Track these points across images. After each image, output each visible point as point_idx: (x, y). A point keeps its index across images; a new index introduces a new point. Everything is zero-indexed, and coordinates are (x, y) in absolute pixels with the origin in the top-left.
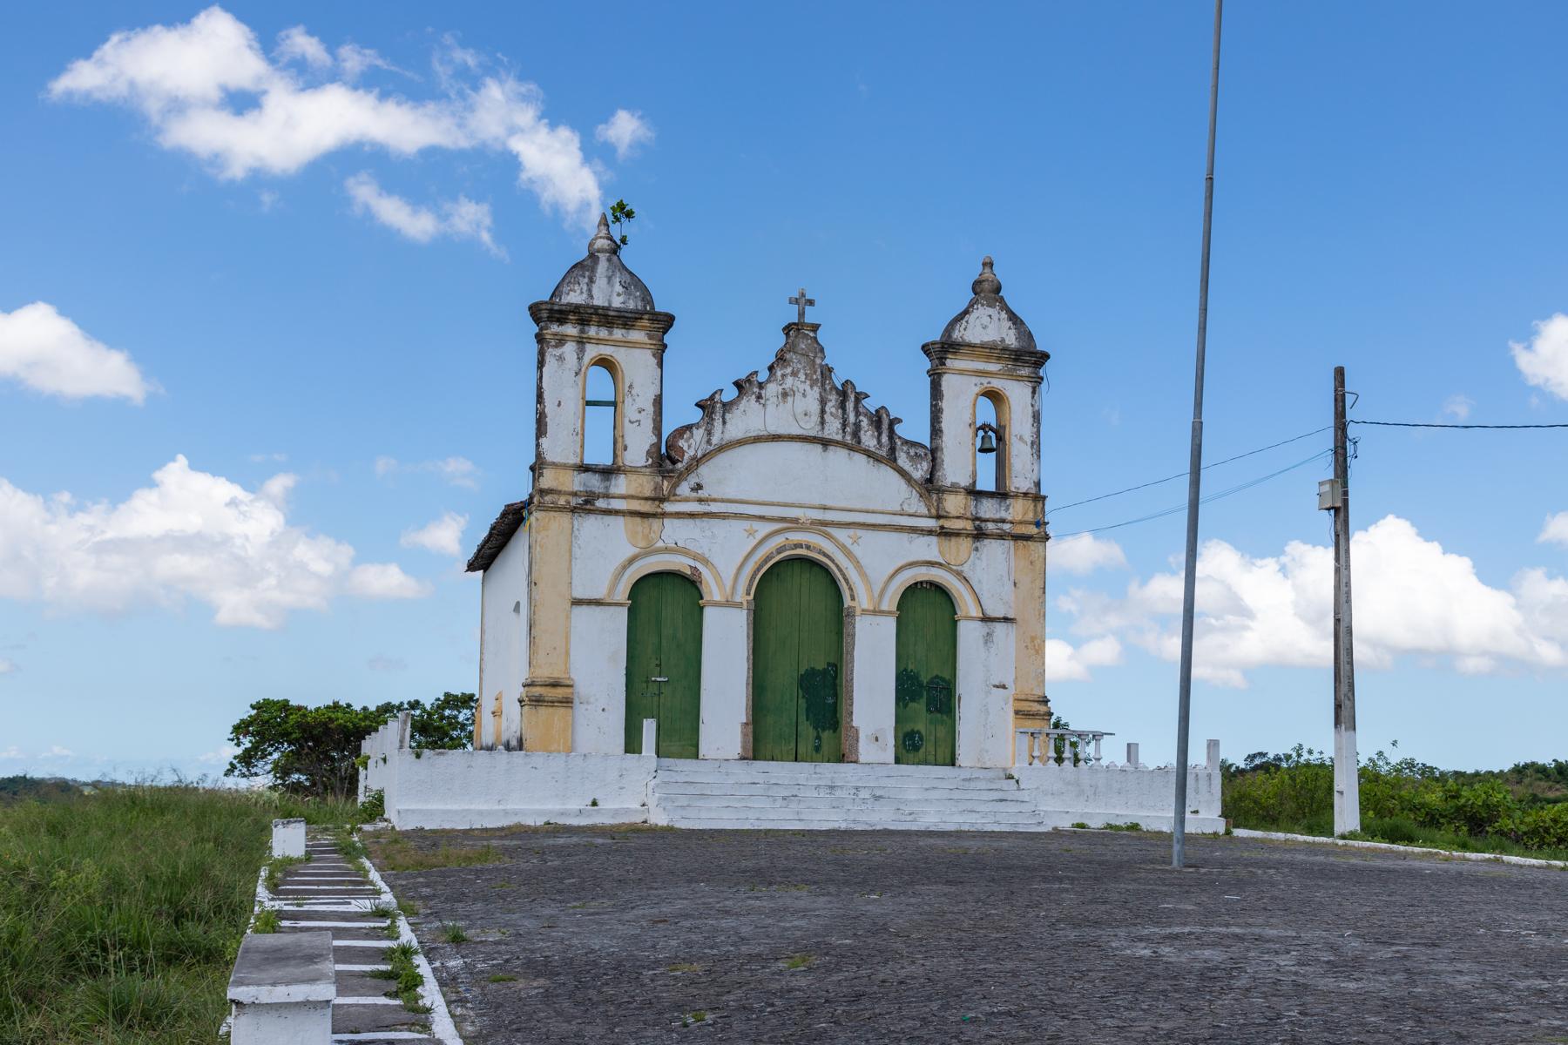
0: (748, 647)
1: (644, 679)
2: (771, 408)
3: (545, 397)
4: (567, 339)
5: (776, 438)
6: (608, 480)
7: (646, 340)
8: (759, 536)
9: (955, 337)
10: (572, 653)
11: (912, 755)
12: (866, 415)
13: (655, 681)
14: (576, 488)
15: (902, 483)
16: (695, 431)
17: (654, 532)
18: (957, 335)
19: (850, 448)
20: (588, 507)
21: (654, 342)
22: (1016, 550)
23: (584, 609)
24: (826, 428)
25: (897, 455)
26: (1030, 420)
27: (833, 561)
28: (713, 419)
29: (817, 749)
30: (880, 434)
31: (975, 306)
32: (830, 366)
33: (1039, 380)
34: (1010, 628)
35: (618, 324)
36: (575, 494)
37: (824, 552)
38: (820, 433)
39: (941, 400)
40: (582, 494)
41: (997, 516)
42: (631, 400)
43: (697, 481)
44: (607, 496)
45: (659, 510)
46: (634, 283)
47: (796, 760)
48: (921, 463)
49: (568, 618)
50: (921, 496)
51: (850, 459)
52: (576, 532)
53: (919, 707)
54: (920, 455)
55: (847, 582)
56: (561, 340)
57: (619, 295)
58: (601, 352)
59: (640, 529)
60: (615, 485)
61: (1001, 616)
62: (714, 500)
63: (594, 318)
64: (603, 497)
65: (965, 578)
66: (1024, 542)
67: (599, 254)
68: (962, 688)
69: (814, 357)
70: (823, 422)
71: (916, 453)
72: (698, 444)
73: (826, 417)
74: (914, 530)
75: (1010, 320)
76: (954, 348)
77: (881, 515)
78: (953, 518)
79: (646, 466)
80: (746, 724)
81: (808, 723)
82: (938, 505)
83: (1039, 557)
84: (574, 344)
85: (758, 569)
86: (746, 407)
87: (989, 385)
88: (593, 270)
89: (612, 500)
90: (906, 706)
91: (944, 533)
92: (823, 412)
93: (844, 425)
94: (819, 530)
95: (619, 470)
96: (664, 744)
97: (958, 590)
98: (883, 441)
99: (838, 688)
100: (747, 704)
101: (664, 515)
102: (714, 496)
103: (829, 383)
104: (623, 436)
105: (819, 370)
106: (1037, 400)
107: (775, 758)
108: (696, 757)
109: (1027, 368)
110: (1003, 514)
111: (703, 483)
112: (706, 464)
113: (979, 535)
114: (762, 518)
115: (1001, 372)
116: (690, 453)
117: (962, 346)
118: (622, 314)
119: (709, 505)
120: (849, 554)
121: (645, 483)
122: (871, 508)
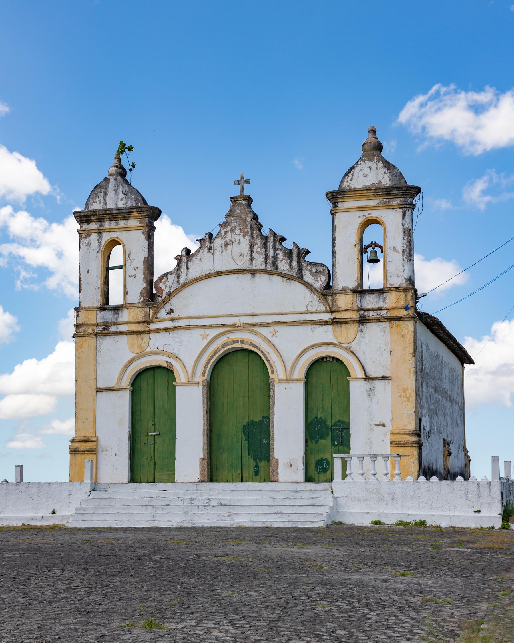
0: (204, 409)
1: (145, 434)
2: (217, 254)
5: (219, 274)
6: (117, 314)
7: (138, 224)
8: (210, 338)
9: (344, 186)
10: (98, 420)
13: (152, 435)
14: (99, 321)
17: (144, 342)
18: (345, 185)
19: (270, 273)
20: (106, 332)
21: (142, 225)
22: (391, 328)
23: (104, 394)
24: (254, 261)
25: (303, 273)
26: (402, 235)
27: (259, 349)
28: (180, 267)
29: (256, 473)
30: (291, 261)
31: (359, 163)
34: (387, 383)
35: (120, 218)
36: (97, 325)
37: (253, 344)
38: (250, 266)
41: (377, 306)
42: (129, 263)
43: (171, 308)
44: (116, 324)
47: (242, 482)
48: (321, 277)
49: (95, 400)
50: (320, 299)
51: (270, 280)
52: (99, 348)
53: (327, 442)
54: (320, 271)
55: (269, 362)
57: (122, 200)
59: (136, 341)
60: (121, 316)
61: (381, 376)
62: (181, 318)
63: (106, 217)
64: (114, 325)
65: (352, 352)
66: (397, 322)
70: (252, 259)
71: (317, 270)
72: (171, 285)
73: (255, 255)
74: (314, 323)
75: (385, 167)
76: (341, 195)
78: (342, 311)
79: (140, 303)
80: (203, 459)
81: (250, 456)
82: (333, 303)
83: (408, 331)
85: (210, 360)
86: (201, 256)
87: (369, 216)
88: (106, 187)
89: (119, 326)
91: (335, 322)
92: (252, 252)
93: (266, 259)
94: (249, 330)
95: (122, 307)
96: (158, 474)
97: (348, 360)
98: (293, 265)
100: (204, 447)
101: (149, 331)
102: (182, 316)
103: (256, 232)
105: (249, 225)
107: (228, 481)
108: (173, 481)
110: (381, 304)
112: (176, 296)
113: (362, 321)
114: (210, 326)
115: (377, 205)
116: (166, 291)
117: (345, 192)
118: (121, 211)
121: (139, 313)
122: (285, 311)
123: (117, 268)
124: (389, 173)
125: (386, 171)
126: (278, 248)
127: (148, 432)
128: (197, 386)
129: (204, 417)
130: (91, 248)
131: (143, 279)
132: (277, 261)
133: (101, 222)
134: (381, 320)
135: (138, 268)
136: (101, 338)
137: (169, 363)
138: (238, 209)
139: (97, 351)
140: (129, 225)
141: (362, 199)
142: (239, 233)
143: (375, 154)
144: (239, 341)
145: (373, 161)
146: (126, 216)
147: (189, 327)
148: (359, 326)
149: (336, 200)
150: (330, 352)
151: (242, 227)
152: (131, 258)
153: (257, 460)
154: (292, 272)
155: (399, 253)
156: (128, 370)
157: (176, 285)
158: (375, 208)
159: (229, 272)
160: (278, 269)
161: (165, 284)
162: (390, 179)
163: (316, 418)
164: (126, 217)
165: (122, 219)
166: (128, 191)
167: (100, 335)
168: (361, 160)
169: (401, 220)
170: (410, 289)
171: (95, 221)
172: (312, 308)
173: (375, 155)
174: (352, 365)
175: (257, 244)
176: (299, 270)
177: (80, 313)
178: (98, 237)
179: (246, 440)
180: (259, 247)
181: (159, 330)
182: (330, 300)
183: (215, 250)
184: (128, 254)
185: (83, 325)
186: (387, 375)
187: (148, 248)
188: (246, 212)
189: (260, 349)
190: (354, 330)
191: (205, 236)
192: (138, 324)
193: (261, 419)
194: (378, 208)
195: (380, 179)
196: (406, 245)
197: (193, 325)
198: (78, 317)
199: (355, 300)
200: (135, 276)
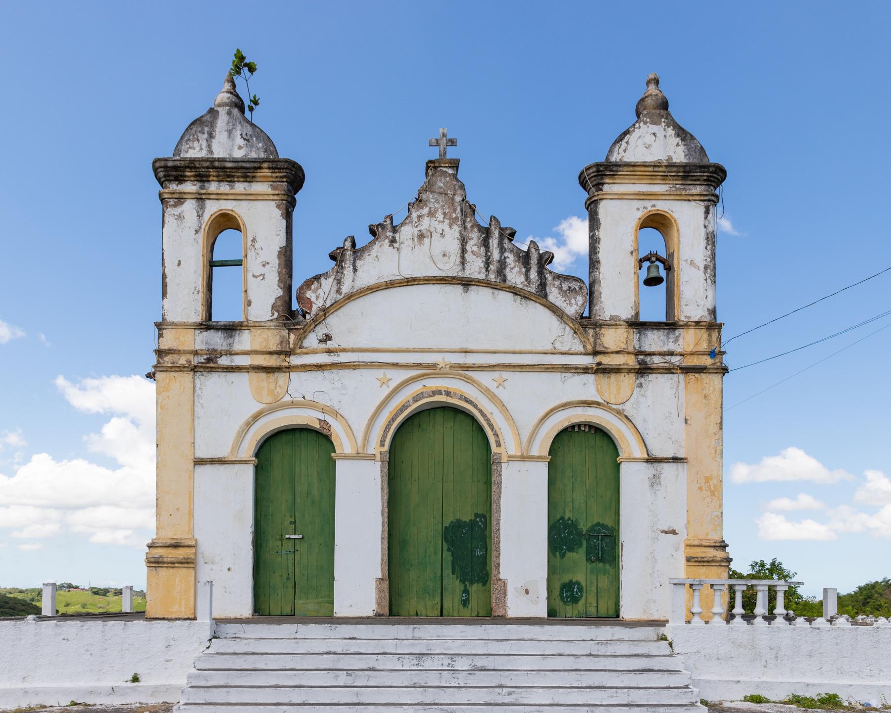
2: (405, 250)
5: (410, 282)
6: (231, 337)
7: (270, 191)
8: (393, 385)
11: (571, 606)
12: (512, 251)
15: (554, 320)
16: (323, 280)
17: (280, 386)
18: (615, 158)
20: (212, 365)
21: (277, 192)
22: (687, 383)
24: (467, 266)
26: (703, 243)
27: (476, 406)
28: (342, 268)
30: (528, 270)
31: (637, 125)
32: (470, 204)
33: (713, 198)
34: (680, 468)
36: (196, 353)
37: (465, 398)
39: (598, 228)
40: (204, 352)
41: (665, 349)
42: (253, 253)
43: (326, 332)
44: (230, 353)
46: (257, 133)
50: (575, 332)
51: (494, 298)
52: (198, 391)
54: (575, 289)
55: (492, 428)
56: (180, 199)
57: (240, 148)
58: (221, 208)
59: (265, 384)
61: (671, 457)
62: (344, 350)
63: (212, 172)
65: (626, 417)
66: (697, 375)
67: (219, 109)
68: (626, 535)
69: (454, 195)
70: (463, 262)
71: (570, 288)
74: (566, 369)
75: (678, 136)
76: (612, 171)
77: (530, 355)
78: (612, 353)
79: (272, 320)
82: (595, 340)
83: (714, 390)
84: (194, 201)
85: (393, 420)
88: (212, 125)
89: (235, 356)
90: (563, 556)
91: (602, 370)
92: (463, 251)
93: (487, 264)
94: (460, 375)
97: (619, 431)
98: (532, 276)
99: (488, 540)
101: (289, 368)
102: (344, 346)
103: (471, 220)
104: (246, 291)
105: (459, 208)
106: (712, 222)
109: (698, 187)
110: (671, 347)
111: (332, 333)
113: (643, 370)
114: (395, 365)
115: (668, 193)
117: (620, 166)
119: (339, 355)
120: (493, 397)
122: (518, 348)
124: (684, 145)
125: (680, 141)
126: (506, 247)
127: (283, 534)
128: (373, 461)
129: (383, 511)
130: (184, 224)
131: (277, 282)
132: (505, 269)
133: (203, 181)
134: (673, 371)
135: (268, 263)
136: (203, 375)
137: (323, 422)
138: (441, 180)
139: (196, 398)
140: (252, 190)
141: (643, 182)
142: (442, 220)
143: (662, 114)
144: (443, 393)
145: (660, 124)
146: (249, 174)
147: (359, 365)
148: (637, 379)
149: (602, 179)
150: (591, 416)
151: (447, 211)
152: (257, 246)
153: (467, 583)
154: (530, 287)
155: (699, 270)
156: (250, 430)
157: (334, 296)
158: (664, 197)
159: (426, 280)
160: (507, 282)
161: (315, 293)
162: (686, 156)
163: (562, 518)
164: (248, 177)
165: (241, 179)
166: (250, 135)
167: (202, 370)
168: (640, 122)
169: (703, 219)
170: (716, 326)
171: (192, 179)
172: (562, 346)
173: (662, 116)
174: (626, 438)
175: (472, 239)
176: (541, 284)
178: (198, 206)
179: (448, 550)
180: (475, 245)
181: (305, 368)
182: (591, 335)
183: (402, 243)
185: (169, 352)
186: (679, 456)
187: (287, 233)
188: (455, 187)
189: (477, 406)
190: (629, 384)
191: (384, 220)
192: (268, 356)
193: (473, 518)
194: (668, 198)
195: (671, 154)
196: (709, 257)
197: (367, 363)
198: (161, 339)
199: (631, 338)
200: (263, 276)
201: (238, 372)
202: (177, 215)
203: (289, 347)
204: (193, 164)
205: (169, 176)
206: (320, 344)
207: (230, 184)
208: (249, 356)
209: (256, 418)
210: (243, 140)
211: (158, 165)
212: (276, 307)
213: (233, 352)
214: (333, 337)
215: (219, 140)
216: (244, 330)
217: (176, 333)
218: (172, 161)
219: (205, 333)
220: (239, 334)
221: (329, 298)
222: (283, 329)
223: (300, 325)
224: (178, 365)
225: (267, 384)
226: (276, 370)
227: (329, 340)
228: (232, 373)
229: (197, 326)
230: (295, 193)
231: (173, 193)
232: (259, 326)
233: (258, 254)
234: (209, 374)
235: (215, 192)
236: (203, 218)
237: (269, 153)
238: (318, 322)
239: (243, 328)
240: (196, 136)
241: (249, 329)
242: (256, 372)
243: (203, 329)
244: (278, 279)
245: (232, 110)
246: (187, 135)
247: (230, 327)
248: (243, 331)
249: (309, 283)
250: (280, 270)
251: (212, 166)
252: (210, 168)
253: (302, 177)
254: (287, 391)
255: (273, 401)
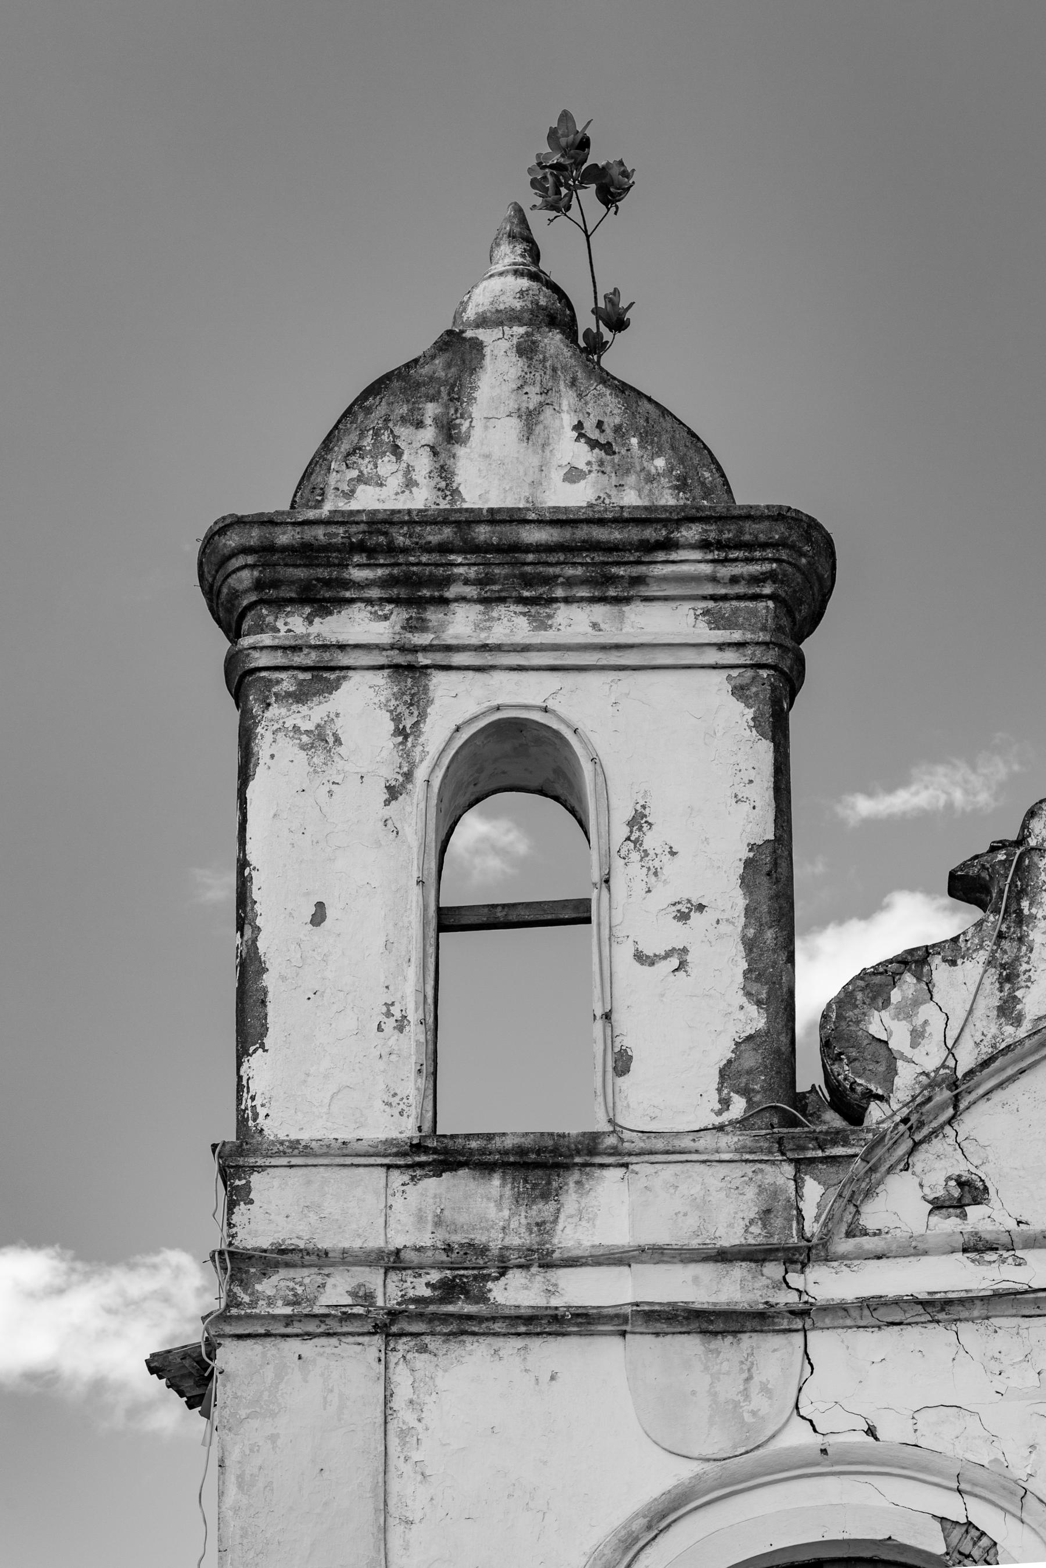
3: (255, 897)
4: (344, 659)
6: (545, 1196)
17: (765, 1389)
20: (461, 1307)
21: (737, 636)
35: (570, 583)
40: (428, 1257)
43: (961, 1168)
45: (786, 1298)
52: (405, 1416)
58: (499, 702)
63: (463, 566)
79: (721, 1128)
84: (380, 679)
89: (562, 1272)
95: (592, 1152)
104: (607, 1016)
112: (998, 1096)
119: (1020, 1263)
123: (528, 916)
131: (740, 979)
135: (701, 908)
136: (423, 1349)
139: (394, 1441)
140: (627, 628)
146: (621, 571)
152: (651, 840)
161: (909, 1017)
164: (611, 580)
165: (583, 592)
166: (617, 429)
171: (375, 593)
177: (255, 1178)
184: (629, 814)
198: (241, 1208)
201: (579, 1334)
202: (307, 732)
203: (801, 1231)
204: (386, 534)
205: (275, 584)
206: (935, 1219)
207: (533, 610)
208: (626, 1269)
209: (664, 1517)
210: (586, 448)
211: (232, 540)
212: (739, 1074)
213: (556, 1255)
214: (992, 1191)
215: (486, 450)
216: (602, 1166)
217: (309, 1183)
218: (295, 524)
219: (431, 1185)
220: (578, 1183)
221: (967, 1031)
222: (773, 1162)
223: (846, 1143)
224: (317, 1310)
225: (708, 1379)
226: (749, 1325)
227: (976, 1202)
228: (550, 1339)
229: (396, 1155)
230: (800, 638)
231: (296, 649)
232: (667, 1152)
233: (656, 874)
234: (453, 1345)
235: (474, 641)
236: (421, 740)
237: (698, 491)
238: (925, 1131)
239: (598, 1160)
240: (385, 437)
241: (626, 1165)
242: (657, 1334)
243: (421, 1165)
244: (745, 966)
245: (537, 337)
246: (347, 431)
247: (544, 1157)
248: (598, 1172)
249: (878, 979)
250: (751, 932)
251: (465, 541)
252: (452, 551)
253: (829, 583)
254: (797, 1408)
255: (735, 1447)
